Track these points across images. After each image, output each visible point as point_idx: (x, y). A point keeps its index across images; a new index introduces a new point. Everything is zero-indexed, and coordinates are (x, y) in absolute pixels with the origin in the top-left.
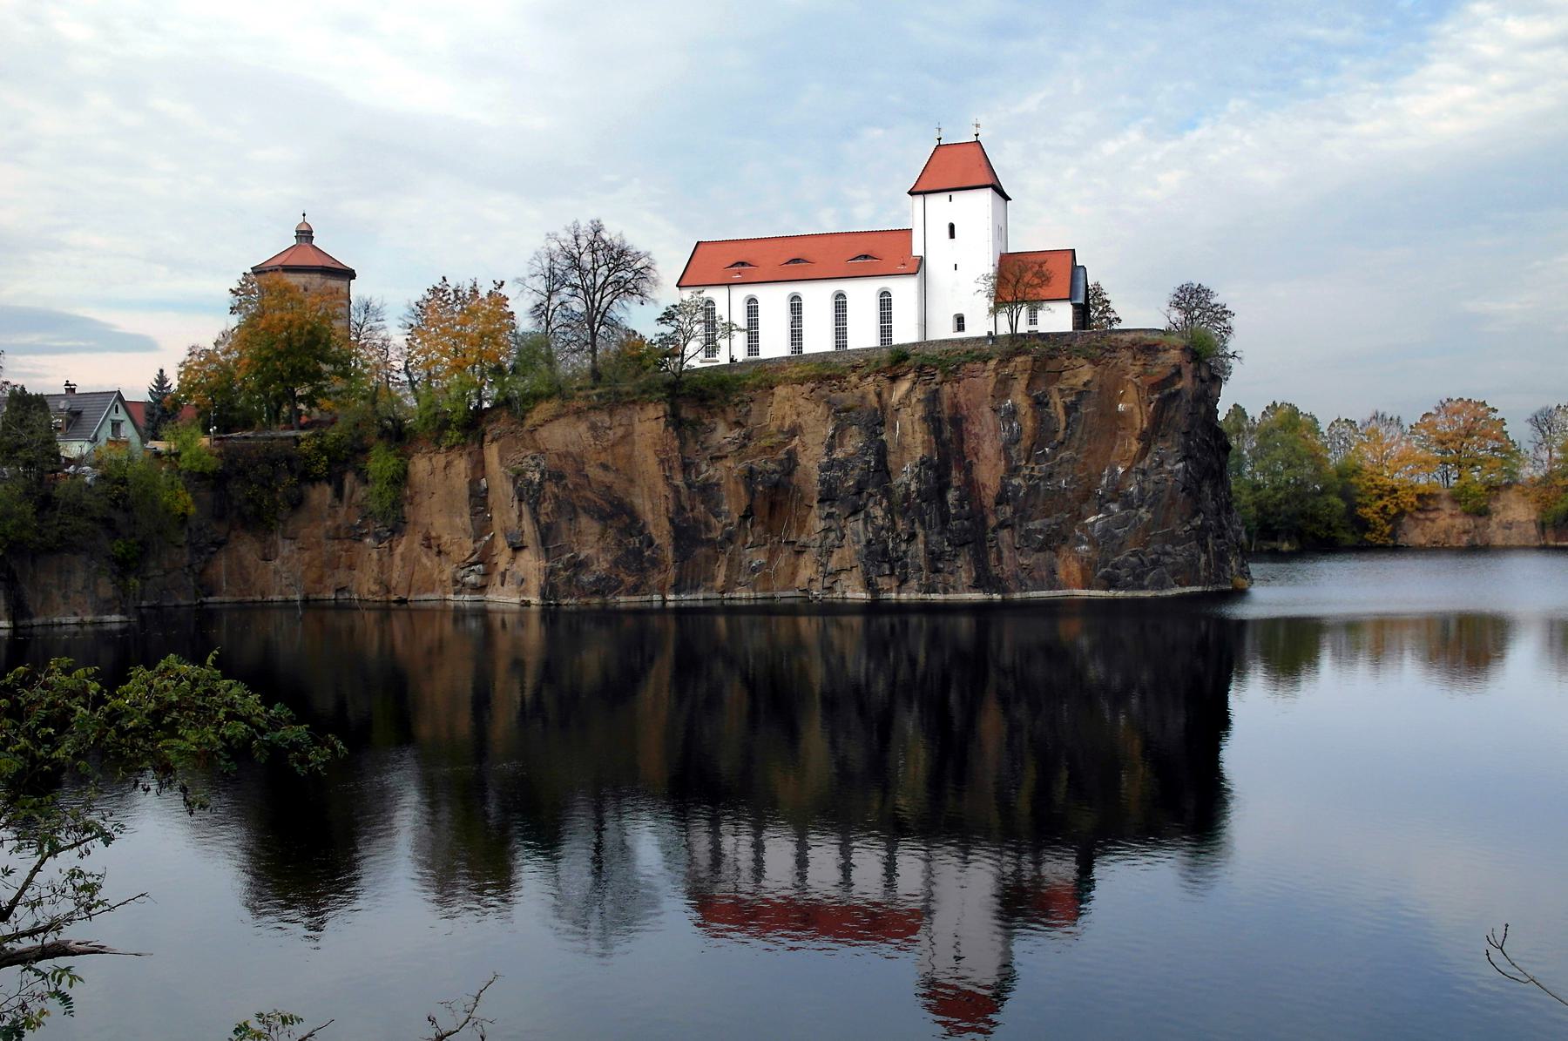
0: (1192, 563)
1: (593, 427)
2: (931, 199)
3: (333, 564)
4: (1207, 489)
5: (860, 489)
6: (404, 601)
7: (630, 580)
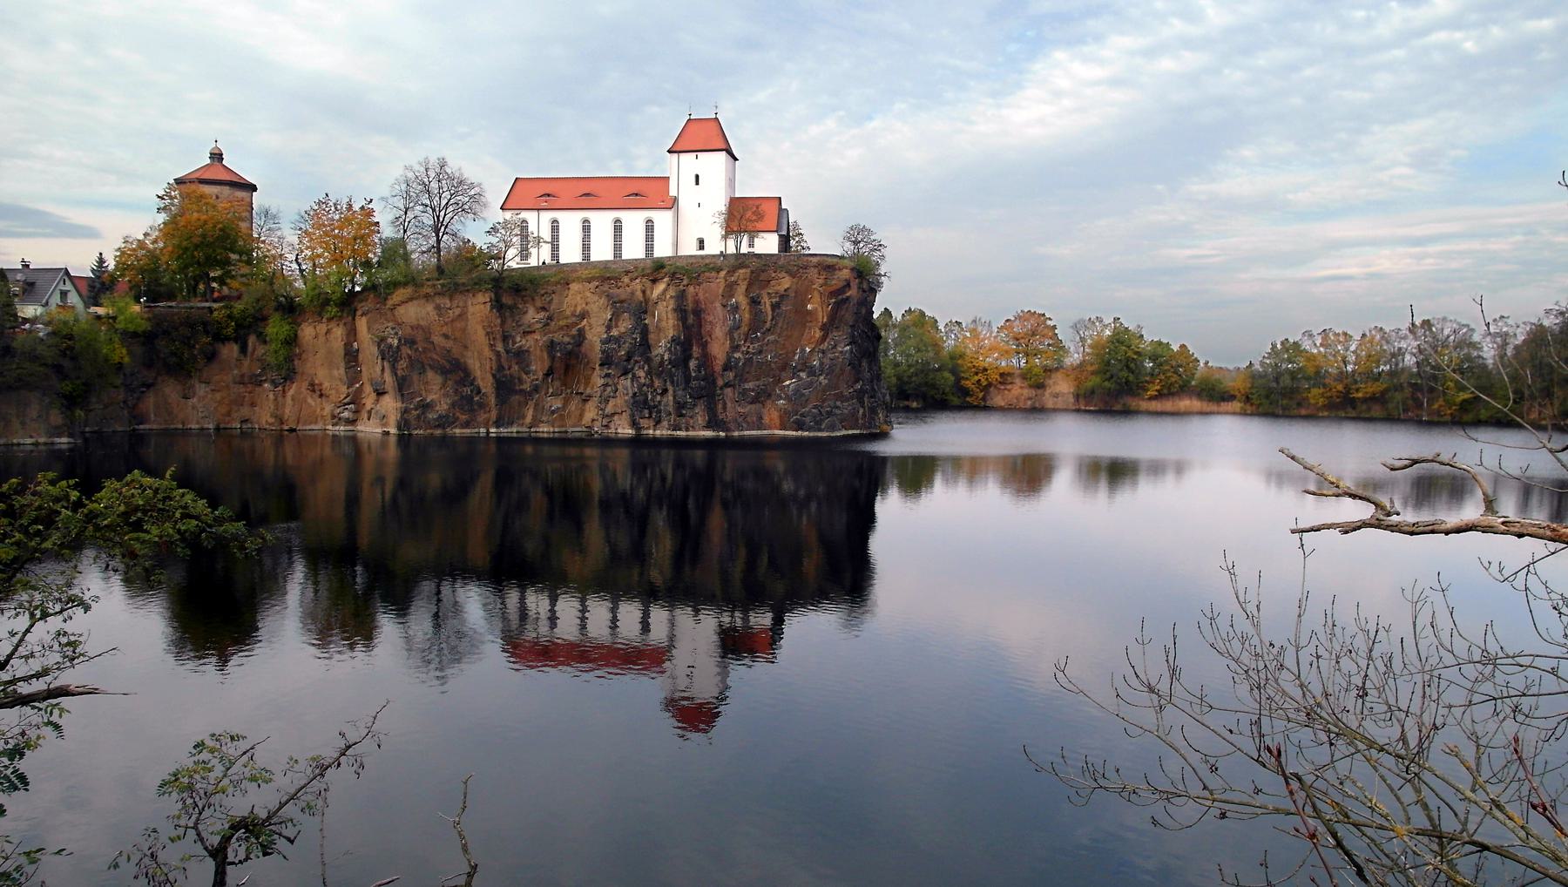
0: (854, 414)
1: (438, 308)
3: (239, 401)
4: (864, 364)
7: (464, 417)
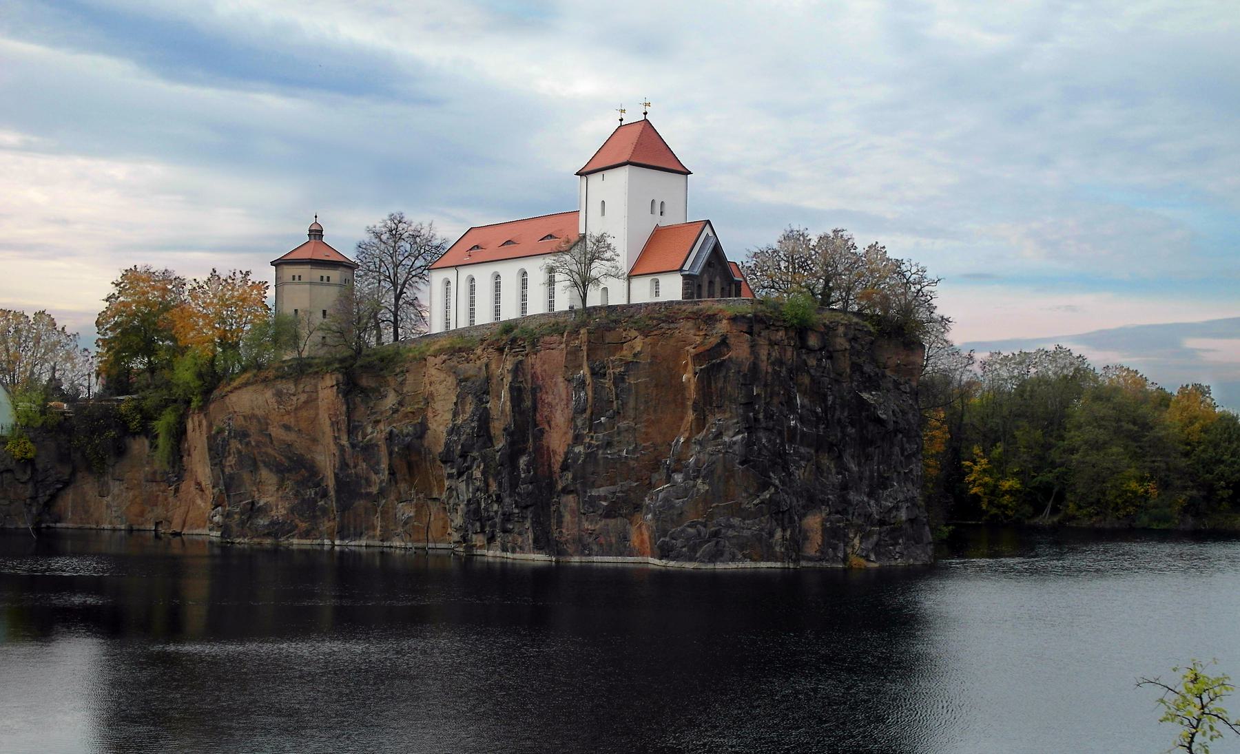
1: (279, 394)
2: (592, 178)
3: (152, 501)
5: (464, 455)
6: (179, 534)
7: (303, 526)
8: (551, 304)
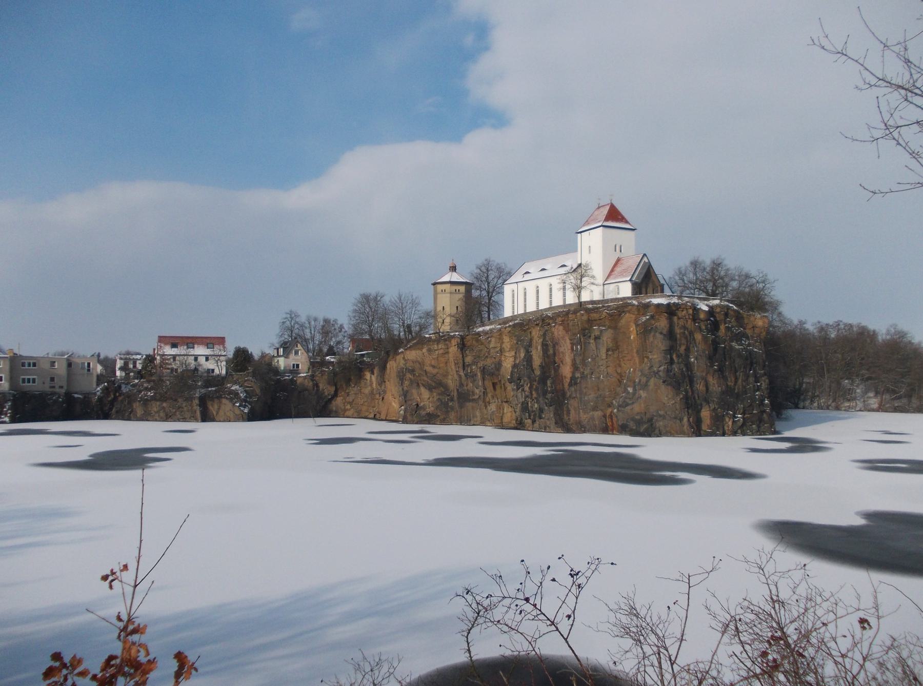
8: (564, 300)
